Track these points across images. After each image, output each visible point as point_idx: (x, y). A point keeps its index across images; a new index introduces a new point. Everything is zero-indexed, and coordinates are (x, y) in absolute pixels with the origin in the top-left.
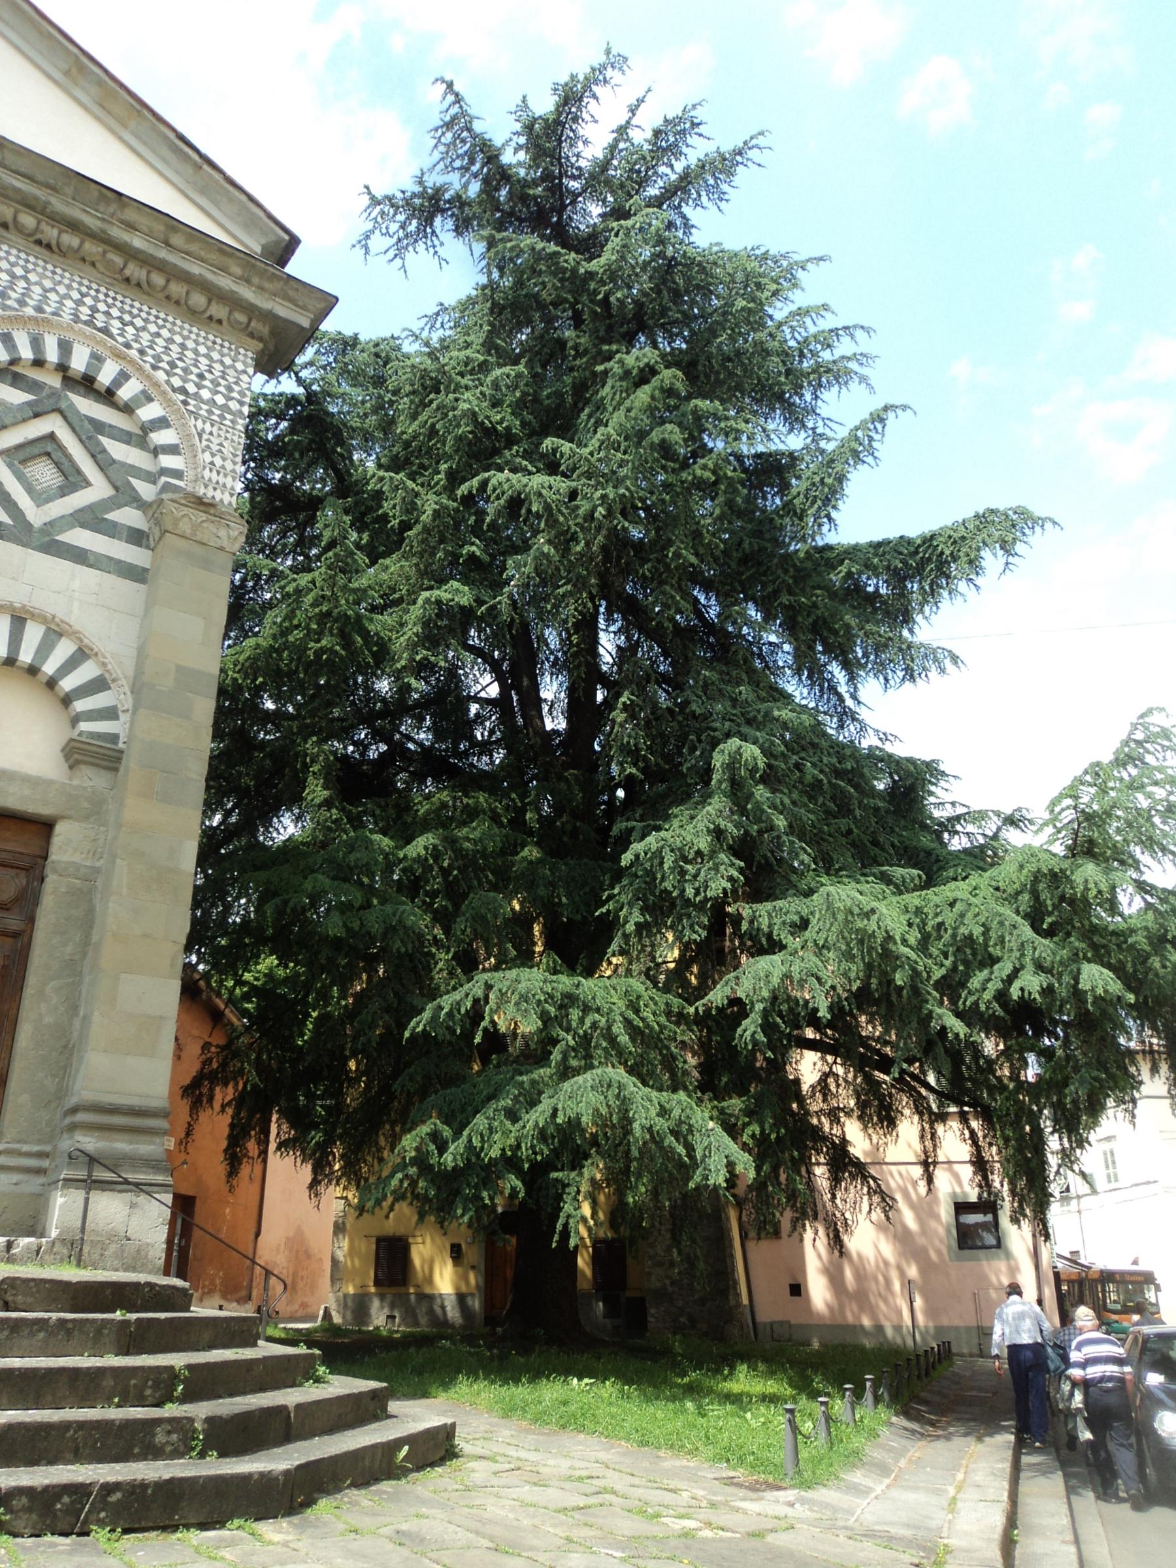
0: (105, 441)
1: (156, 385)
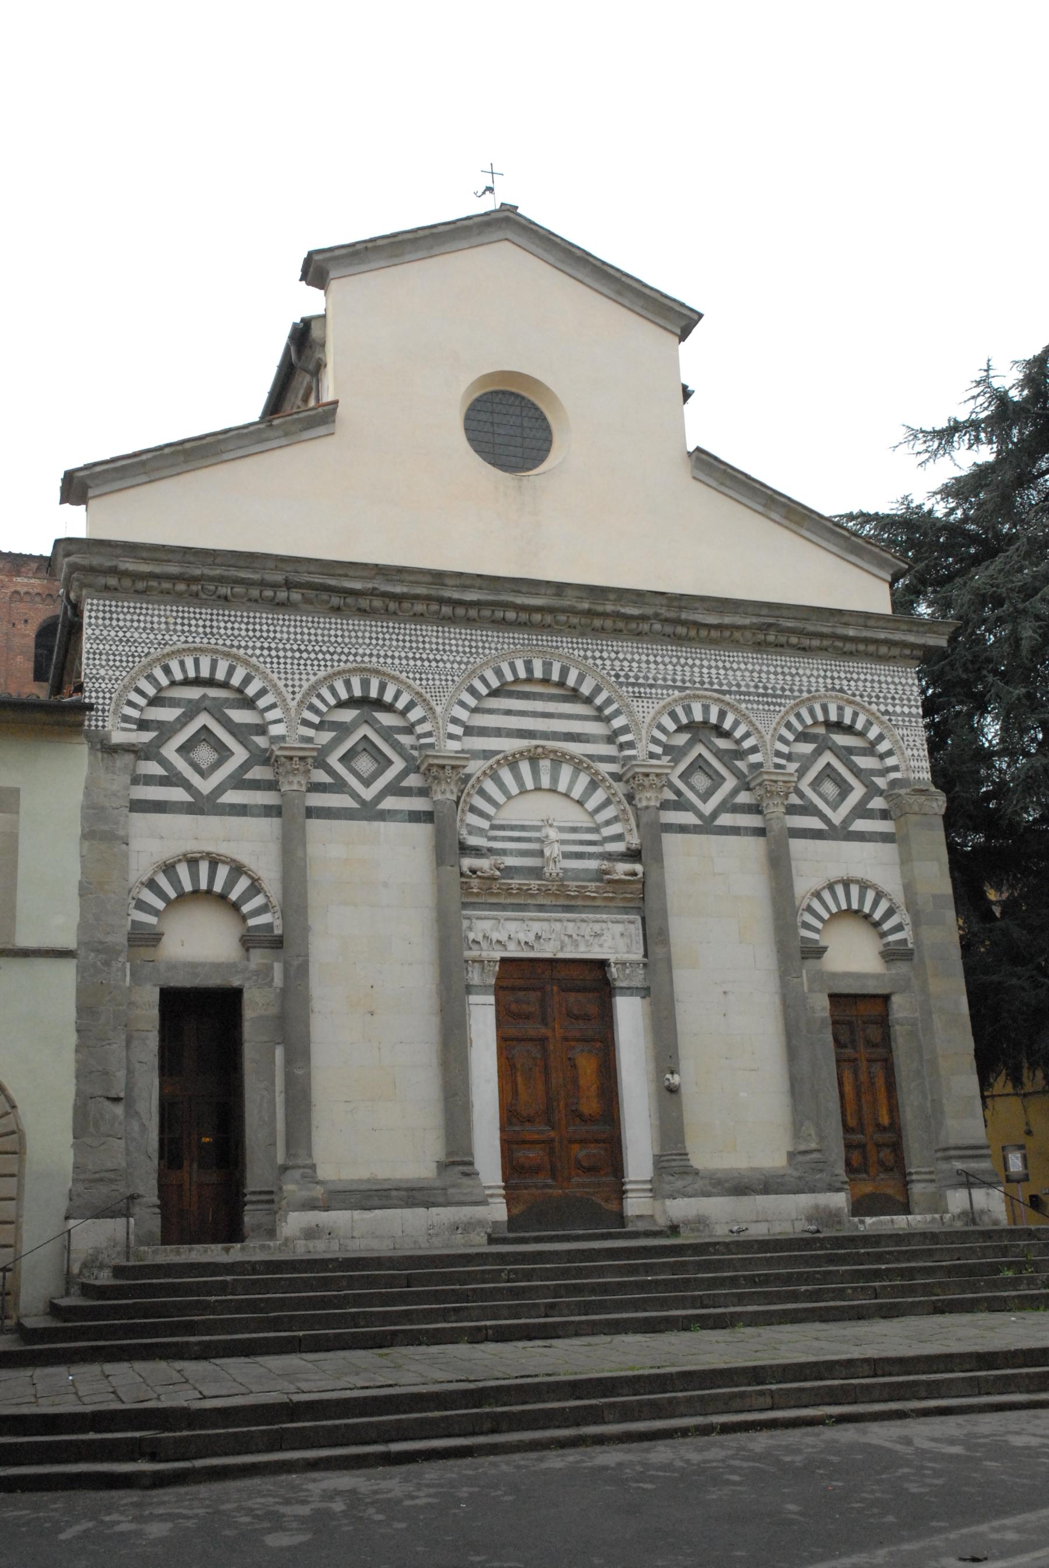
0: (854, 758)
1: (873, 714)
